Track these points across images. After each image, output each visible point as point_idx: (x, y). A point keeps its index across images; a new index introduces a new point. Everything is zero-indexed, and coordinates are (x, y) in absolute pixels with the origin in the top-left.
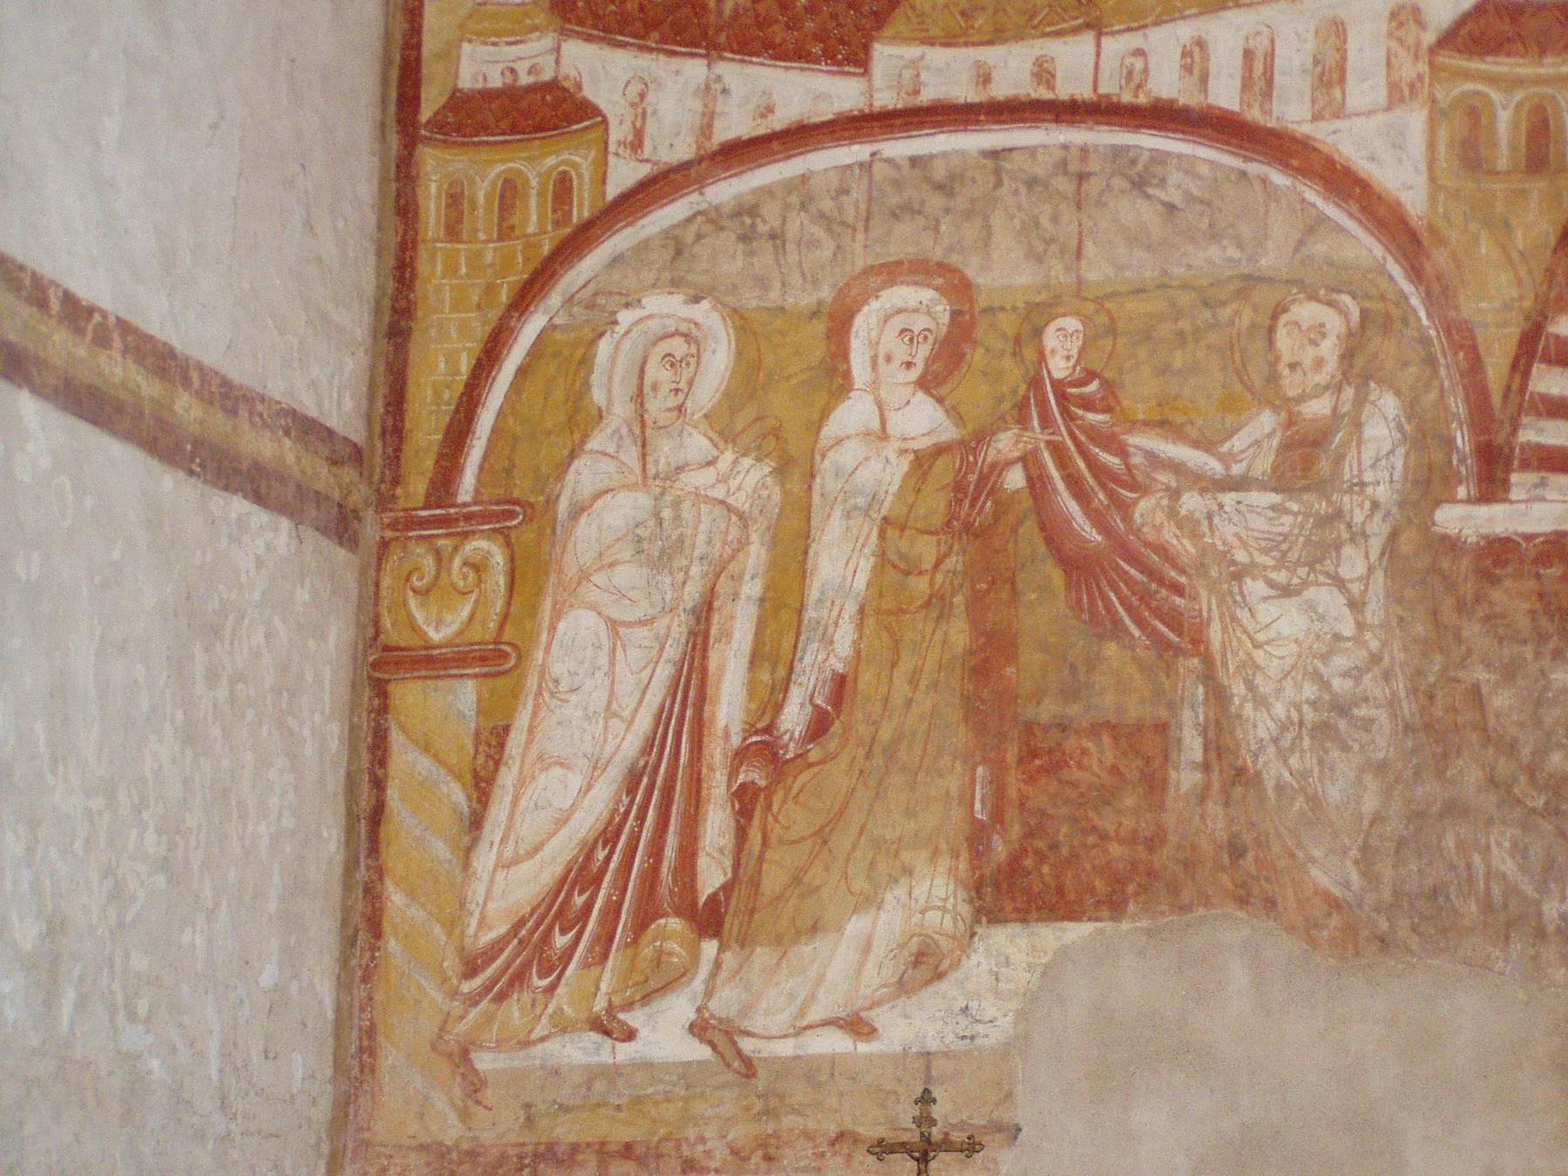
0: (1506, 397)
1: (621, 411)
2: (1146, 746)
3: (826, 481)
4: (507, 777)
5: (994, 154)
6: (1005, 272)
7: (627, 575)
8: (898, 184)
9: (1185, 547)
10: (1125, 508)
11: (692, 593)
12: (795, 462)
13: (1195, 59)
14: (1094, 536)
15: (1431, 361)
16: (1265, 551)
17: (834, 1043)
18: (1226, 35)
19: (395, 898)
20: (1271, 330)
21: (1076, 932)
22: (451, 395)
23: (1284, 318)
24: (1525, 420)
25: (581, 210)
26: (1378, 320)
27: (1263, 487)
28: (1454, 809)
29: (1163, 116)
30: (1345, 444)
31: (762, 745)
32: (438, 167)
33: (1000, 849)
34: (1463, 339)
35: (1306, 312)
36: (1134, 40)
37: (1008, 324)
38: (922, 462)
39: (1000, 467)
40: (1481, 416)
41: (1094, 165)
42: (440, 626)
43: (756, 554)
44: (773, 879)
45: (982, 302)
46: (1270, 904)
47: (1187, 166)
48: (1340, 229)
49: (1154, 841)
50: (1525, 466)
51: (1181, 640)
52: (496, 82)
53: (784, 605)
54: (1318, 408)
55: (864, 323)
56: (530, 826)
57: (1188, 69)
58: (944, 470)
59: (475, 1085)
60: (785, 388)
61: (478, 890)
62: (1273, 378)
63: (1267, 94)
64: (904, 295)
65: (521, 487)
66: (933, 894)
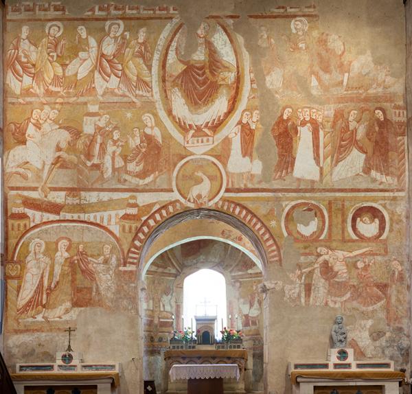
1: (33, 251)
2: (90, 289)
3: (56, 261)
4: (21, 291)
6: (75, 239)
7: (34, 270)
9: (94, 270)
11: (41, 272)
12: (53, 259)
13: (95, 217)
17: (58, 319)
18: (98, 215)
19: (9, 303)
21: (82, 309)
22: (14, 248)
25: (28, 228)
28: (120, 298)
31: (49, 288)
32: (10, 222)
33: (75, 300)
34: (122, 250)
36: (89, 214)
38: (66, 259)
40: (124, 259)
42: (13, 274)
43: (48, 268)
44: (51, 302)
46: (102, 306)
47: (94, 229)
49: (91, 299)
51: (93, 279)
52: (17, 212)
53: (51, 274)
54: (108, 256)
55: (60, 244)
56: (24, 296)
58: (69, 260)
59: (19, 323)
60: (51, 250)
61: (18, 303)
64: (64, 241)
65: (22, 259)
66: (68, 304)
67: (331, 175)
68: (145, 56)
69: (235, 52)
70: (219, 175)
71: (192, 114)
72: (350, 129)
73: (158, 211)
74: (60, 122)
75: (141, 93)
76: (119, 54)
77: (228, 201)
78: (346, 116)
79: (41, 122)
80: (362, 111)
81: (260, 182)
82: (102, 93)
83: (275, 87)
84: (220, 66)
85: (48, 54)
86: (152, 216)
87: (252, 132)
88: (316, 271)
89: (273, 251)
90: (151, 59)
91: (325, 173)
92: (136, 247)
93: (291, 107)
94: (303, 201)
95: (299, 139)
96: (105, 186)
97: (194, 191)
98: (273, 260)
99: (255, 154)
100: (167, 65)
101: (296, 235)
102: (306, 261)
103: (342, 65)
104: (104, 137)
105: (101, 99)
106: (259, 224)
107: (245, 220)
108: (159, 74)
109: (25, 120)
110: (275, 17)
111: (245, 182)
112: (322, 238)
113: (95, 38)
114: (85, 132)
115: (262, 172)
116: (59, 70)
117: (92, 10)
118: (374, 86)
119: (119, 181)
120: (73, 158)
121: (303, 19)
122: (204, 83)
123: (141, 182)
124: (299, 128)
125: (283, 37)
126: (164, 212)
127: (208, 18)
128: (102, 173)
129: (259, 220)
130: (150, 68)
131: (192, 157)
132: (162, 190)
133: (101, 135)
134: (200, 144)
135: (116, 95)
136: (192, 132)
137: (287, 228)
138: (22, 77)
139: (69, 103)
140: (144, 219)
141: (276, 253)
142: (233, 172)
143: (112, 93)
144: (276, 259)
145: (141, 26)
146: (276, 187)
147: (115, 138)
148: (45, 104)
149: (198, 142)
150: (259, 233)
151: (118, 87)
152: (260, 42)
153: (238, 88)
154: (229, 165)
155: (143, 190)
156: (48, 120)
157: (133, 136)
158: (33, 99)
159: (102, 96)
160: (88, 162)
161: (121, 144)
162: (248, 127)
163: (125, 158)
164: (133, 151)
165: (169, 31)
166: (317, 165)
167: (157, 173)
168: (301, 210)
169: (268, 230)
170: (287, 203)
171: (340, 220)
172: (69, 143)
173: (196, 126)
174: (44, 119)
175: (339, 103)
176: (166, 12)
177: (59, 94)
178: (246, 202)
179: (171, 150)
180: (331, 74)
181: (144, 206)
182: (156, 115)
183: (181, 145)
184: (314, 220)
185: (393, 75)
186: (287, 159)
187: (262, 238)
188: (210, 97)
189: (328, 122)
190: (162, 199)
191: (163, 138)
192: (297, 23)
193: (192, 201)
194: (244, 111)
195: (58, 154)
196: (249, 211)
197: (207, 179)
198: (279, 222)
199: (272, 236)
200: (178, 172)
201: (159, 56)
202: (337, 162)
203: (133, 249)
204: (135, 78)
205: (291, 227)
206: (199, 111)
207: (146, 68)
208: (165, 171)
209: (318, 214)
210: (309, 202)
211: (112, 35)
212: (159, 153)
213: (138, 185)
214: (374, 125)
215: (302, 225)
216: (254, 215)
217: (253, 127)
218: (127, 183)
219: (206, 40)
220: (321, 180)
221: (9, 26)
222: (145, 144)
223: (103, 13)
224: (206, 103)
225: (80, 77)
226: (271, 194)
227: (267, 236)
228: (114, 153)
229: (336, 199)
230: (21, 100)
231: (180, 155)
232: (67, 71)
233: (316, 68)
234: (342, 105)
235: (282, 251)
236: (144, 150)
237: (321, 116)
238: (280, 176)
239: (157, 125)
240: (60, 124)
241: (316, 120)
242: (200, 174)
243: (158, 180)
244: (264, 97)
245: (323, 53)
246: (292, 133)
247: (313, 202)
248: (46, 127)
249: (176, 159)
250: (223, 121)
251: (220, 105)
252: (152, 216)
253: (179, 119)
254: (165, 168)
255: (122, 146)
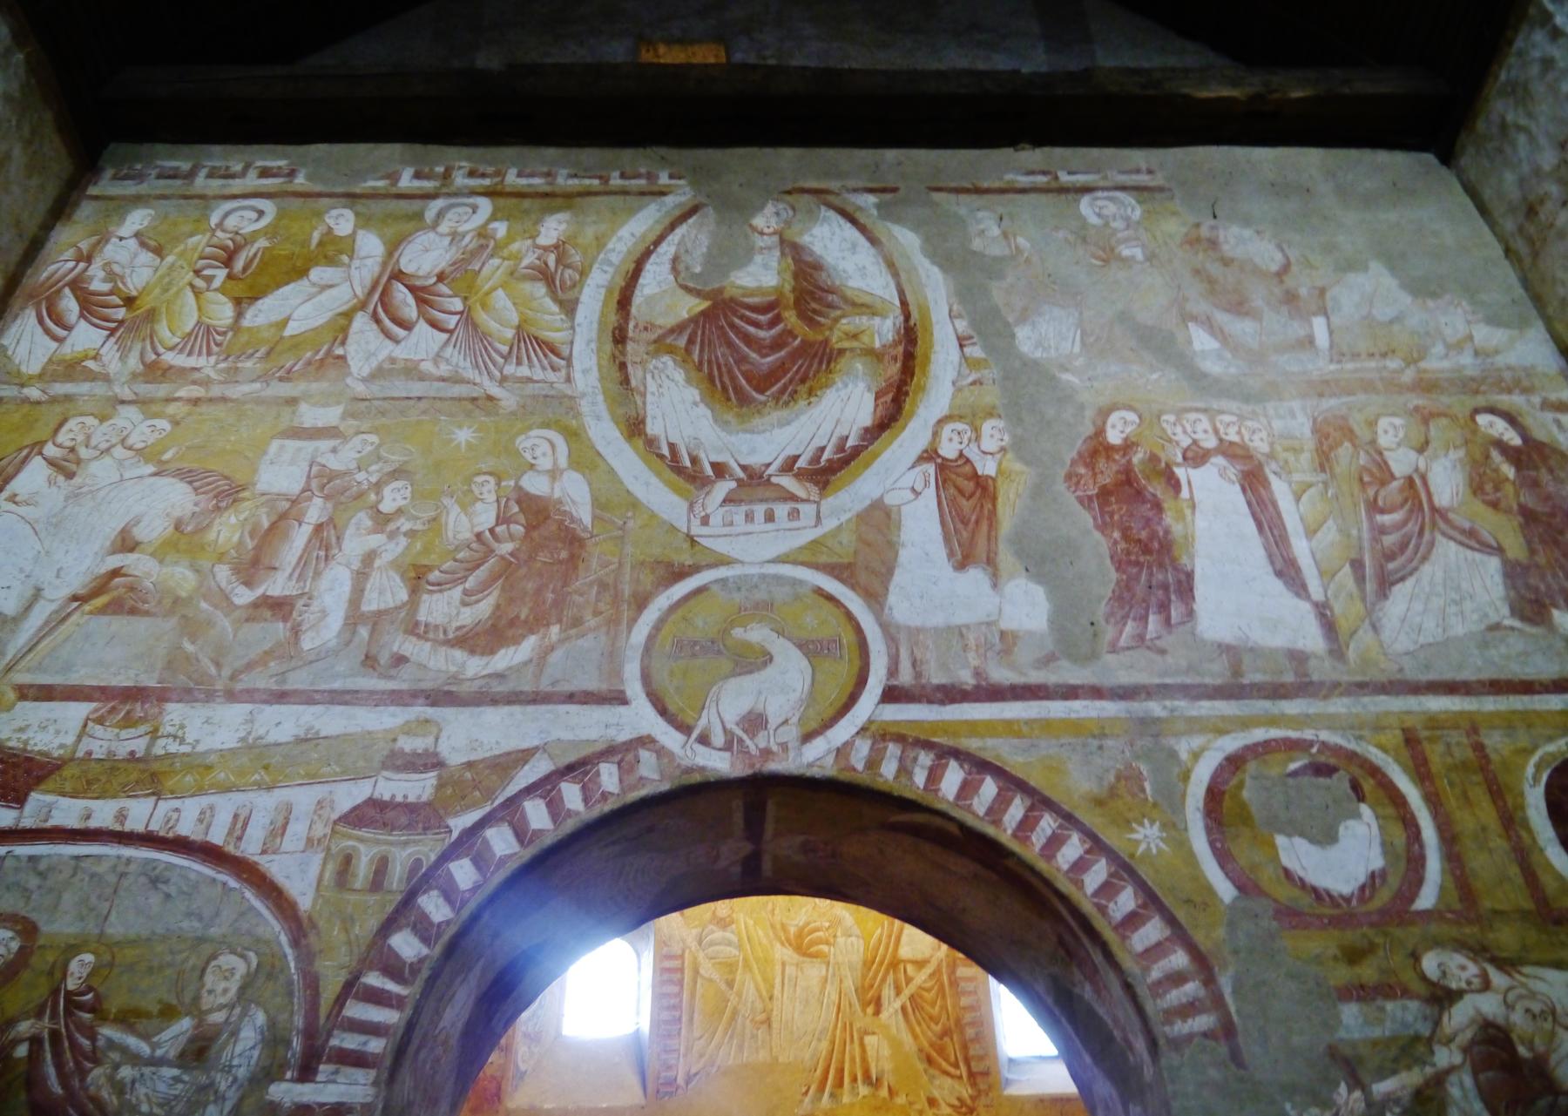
0: (328, 1017)
5: (77, 858)
6: (59, 926)
8: (16, 869)
10: (83, 1073)
13: (205, 818)
14: (58, 1090)
15: (290, 994)
16: (161, 1105)
18: (225, 806)
20: (203, 971)
23: (213, 963)
24: (336, 1032)
26: (269, 969)
27: (170, 1064)
29: (180, 845)
30: (228, 1040)
34: (312, 984)
35: (227, 960)
37: (50, 957)
39: (16, 1042)
40: (310, 1033)
41: (132, 867)
45: (41, 941)
48: (259, 914)
50: (329, 1061)
54: (218, 1017)
57: (201, 821)
62: (197, 999)
63: (240, 838)
67: (1375, 628)
68: (558, 278)
69: (891, 266)
70: (848, 637)
71: (730, 433)
72: (1397, 474)
73: (545, 787)
74: (166, 457)
75: (524, 371)
76: (460, 275)
77: (900, 738)
78: (1362, 433)
79: (84, 453)
80: (1426, 417)
81: (1048, 660)
82: (366, 372)
83: (1053, 353)
84: (842, 304)
85: (197, 273)
86: (510, 811)
87: (983, 488)
88: (1455, 1092)
89: (1177, 979)
90: (577, 285)
91: (1344, 625)
92: (394, 968)
93: (1130, 408)
94: (1275, 733)
95: (1193, 507)
96: (298, 680)
97: (731, 702)
98: (1182, 1027)
99: (1006, 557)
100: (638, 299)
101: (1284, 893)
102: (1376, 1033)
103: (1291, 298)
104: (335, 507)
105: (360, 389)
106: (1075, 838)
107: (997, 823)
108: (600, 323)
109: (21, 449)
110: (1023, 191)
111: (973, 659)
112: (1426, 899)
113: (381, 237)
114: (261, 486)
115: (1051, 622)
116: (223, 312)
117: (394, 177)
118: (1439, 349)
119: (370, 661)
120: (181, 577)
121: (1118, 194)
122: (776, 345)
123: (475, 666)
124: (1180, 472)
125: (1061, 234)
126: (571, 794)
127: (789, 193)
128: (296, 632)
129: (1068, 819)
130: (569, 308)
131: (722, 572)
132: (571, 698)
133: (327, 498)
134: (759, 524)
135: (422, 377)
136: (724, 488)
137: (1223, 858)
138: (68, 328)
139: (224, 399)
140: (461, 822)
141: (1192, 988)
142: (916, 622)
143: (411, 371)
144: (1203, 1022)
145: (553, 211)
146: (1125, 678)
147: (387, 506)
148: (123, 402)
149: (749, 517)
150: (1080, 885)
151: (438, 355)
152: (977, 244)
153: (909, 357)
154: (893, 599)
155: (484, 698)
156: (119, 452)
157: (468, 501)
158: (85, 387)
159: (364, 380)
160: (242, 589)
161: (405, 525)
162: (967, 468)
163: (417, 578)
164: (457, 549)
165: (651, 222)
166: (1298, 595)
167: (555, 630)
168: (1275, 771)
169: (1124, 869)
170: (1197, 741)
171: (1487, 814)
172: (178, 526)
173: (744, 468)
174: (104, 446)
175: (1321, 395)
176: (643, 182)
177: (196, 375)
178: (990, 742)
179: (629, 549)
180: (1261, 320)
181: (470, 765)
182: (574, 435)
183: (673, 529)
184: (1357, 815)
185: (1493, 321)
186: (1153, 570)
187: (1103, 910)
188: (803, 381)
189: (1297, 451)
190: (567, 736)
191: (597, 503)
192: (1100, 203)
193: (718, 739)
194: (941, 422)
195: (114, 562)
196: (1012, 783)
197: (796, 654)
198: (1174, 829)
199: (1151, 901)
200: (658, 627)
201: (608, 277)
202: (1385, 583)
203: (374, 979)
204: (509, 334)
205: (1244, 853)
206: (757, 421)
207: (555, 308)
208: (591, 622)
209: (1368, 785)
210: (1308, 734)
211: (444, 227)
212: (573, 561)
213: (455, 679)
214: (1488, 457)
215: (1301, 844)
216: (1040, 802)
217: (987, 468)
218: (406, 672)
219: (782, 241)
220: (1337, 652)
221: (86, 210)
222: (518, 529)
223: (428, 185)
224: (787, 397)
225: (291, 329)
226: (1110, 708)
227: (1126, 901)
228: (369, 558)
229: (1434, 723)
230: (33, 393)
231: (670, 565)
232: (249, 314)
233: (1200, 306)
234: (1333, 402)
235: (1225, 983)
236: (506, 548)
237: (1264, 434)
238: (1140, 638)
239: (576, 463)
240: (160, 462)
241: (1245, 447)
242: (757, 634)
243: (555, 657)
244: (1022, 389)
245: (1215, 269)
246: (1156, 488)
247: (1325, 736)
248: (100, 471)
249: (647, 579)
250: (857, 451)
251: (847, 404)
252: (510, 811)
253: (672, 447)
254: (596, 613)
255: (411, 534)
